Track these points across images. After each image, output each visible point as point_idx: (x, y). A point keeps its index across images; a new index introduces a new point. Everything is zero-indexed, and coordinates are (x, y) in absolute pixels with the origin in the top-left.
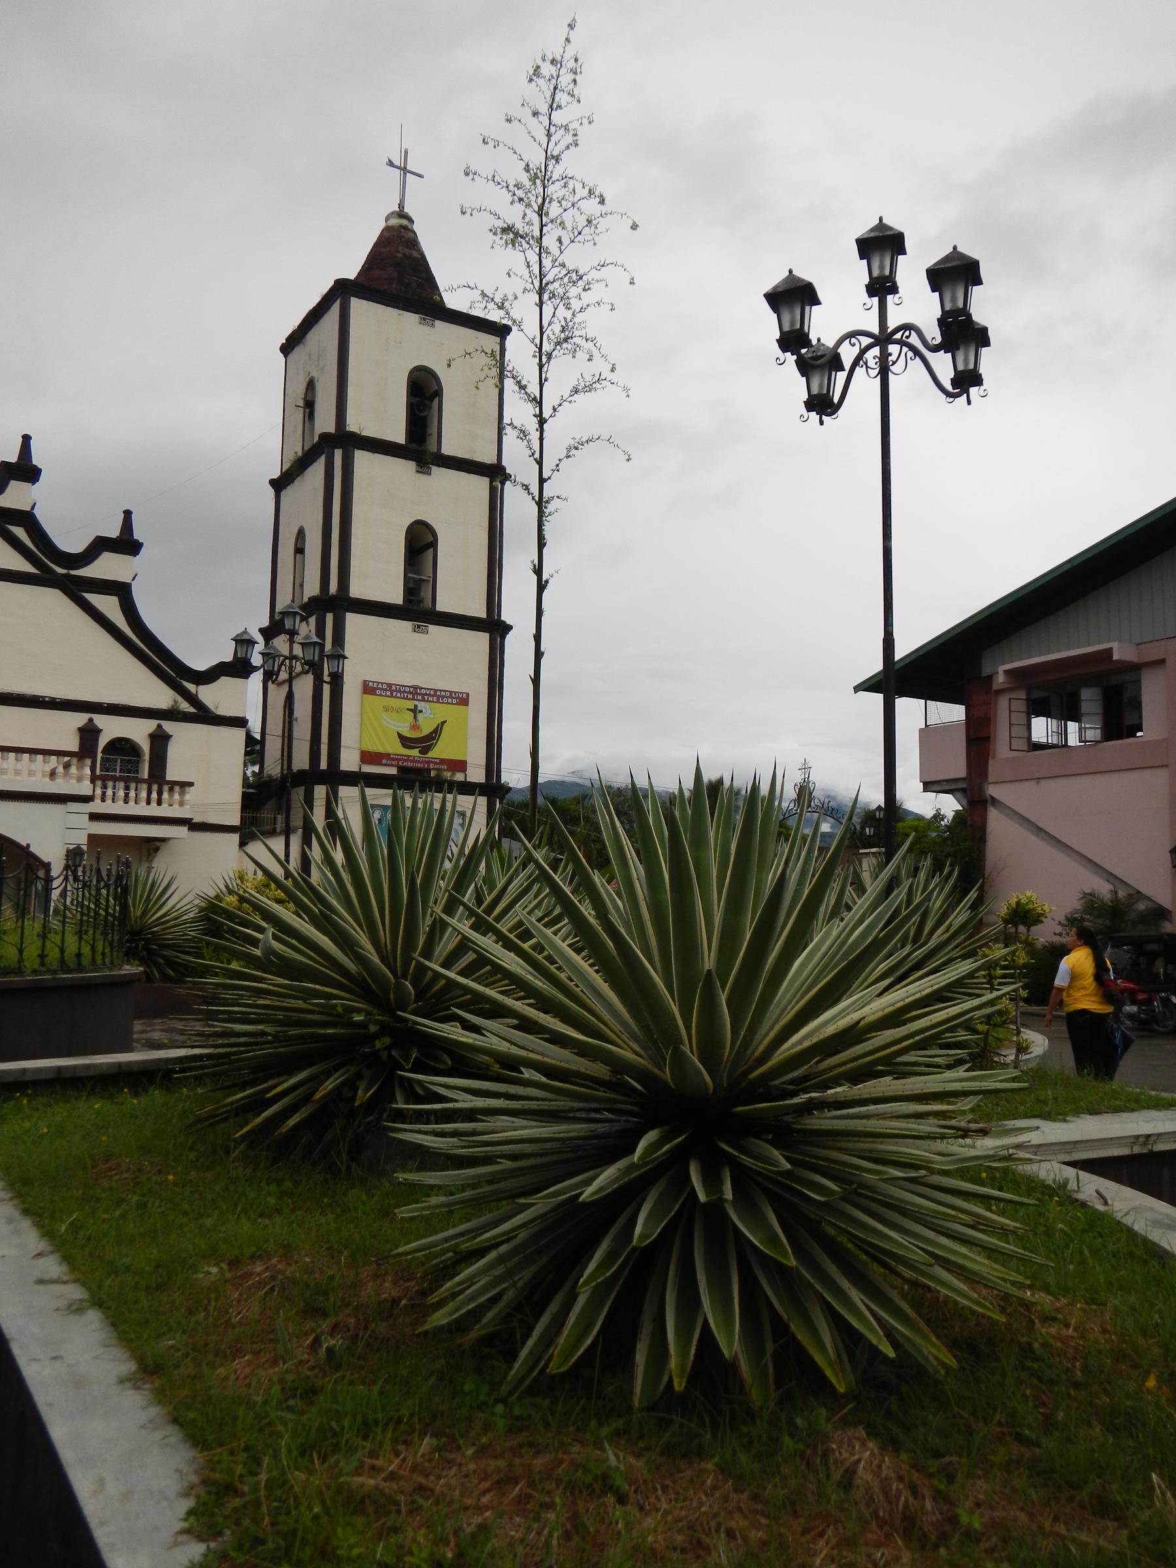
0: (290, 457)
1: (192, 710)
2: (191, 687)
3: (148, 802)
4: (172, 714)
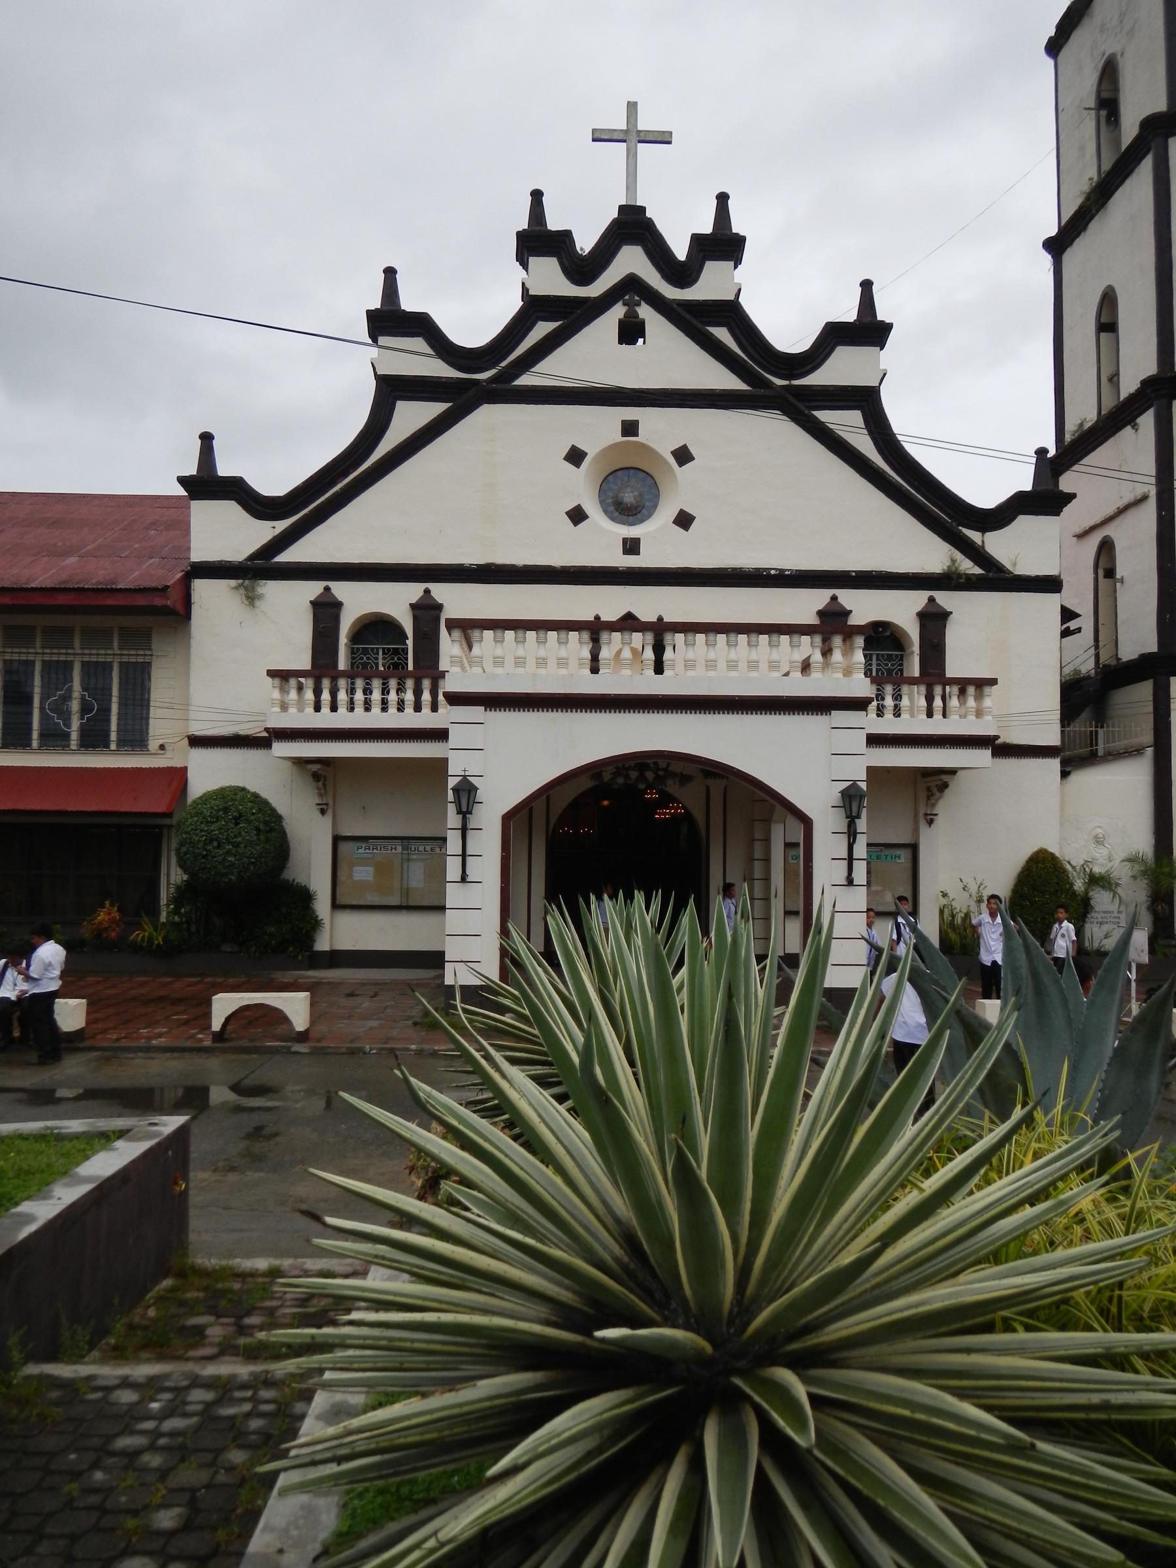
1: (978, 571)
2: (975, 536)
3: (930, 714)
4: (948, 581)
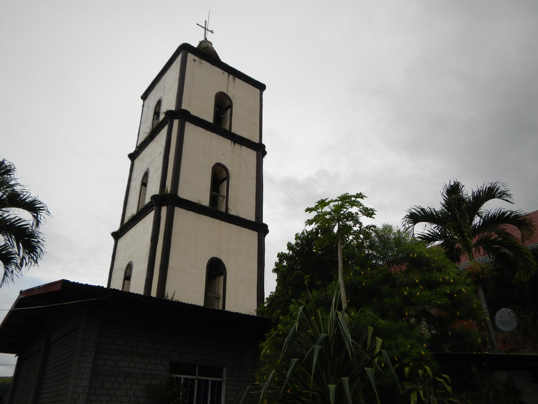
0: (142, 139)
